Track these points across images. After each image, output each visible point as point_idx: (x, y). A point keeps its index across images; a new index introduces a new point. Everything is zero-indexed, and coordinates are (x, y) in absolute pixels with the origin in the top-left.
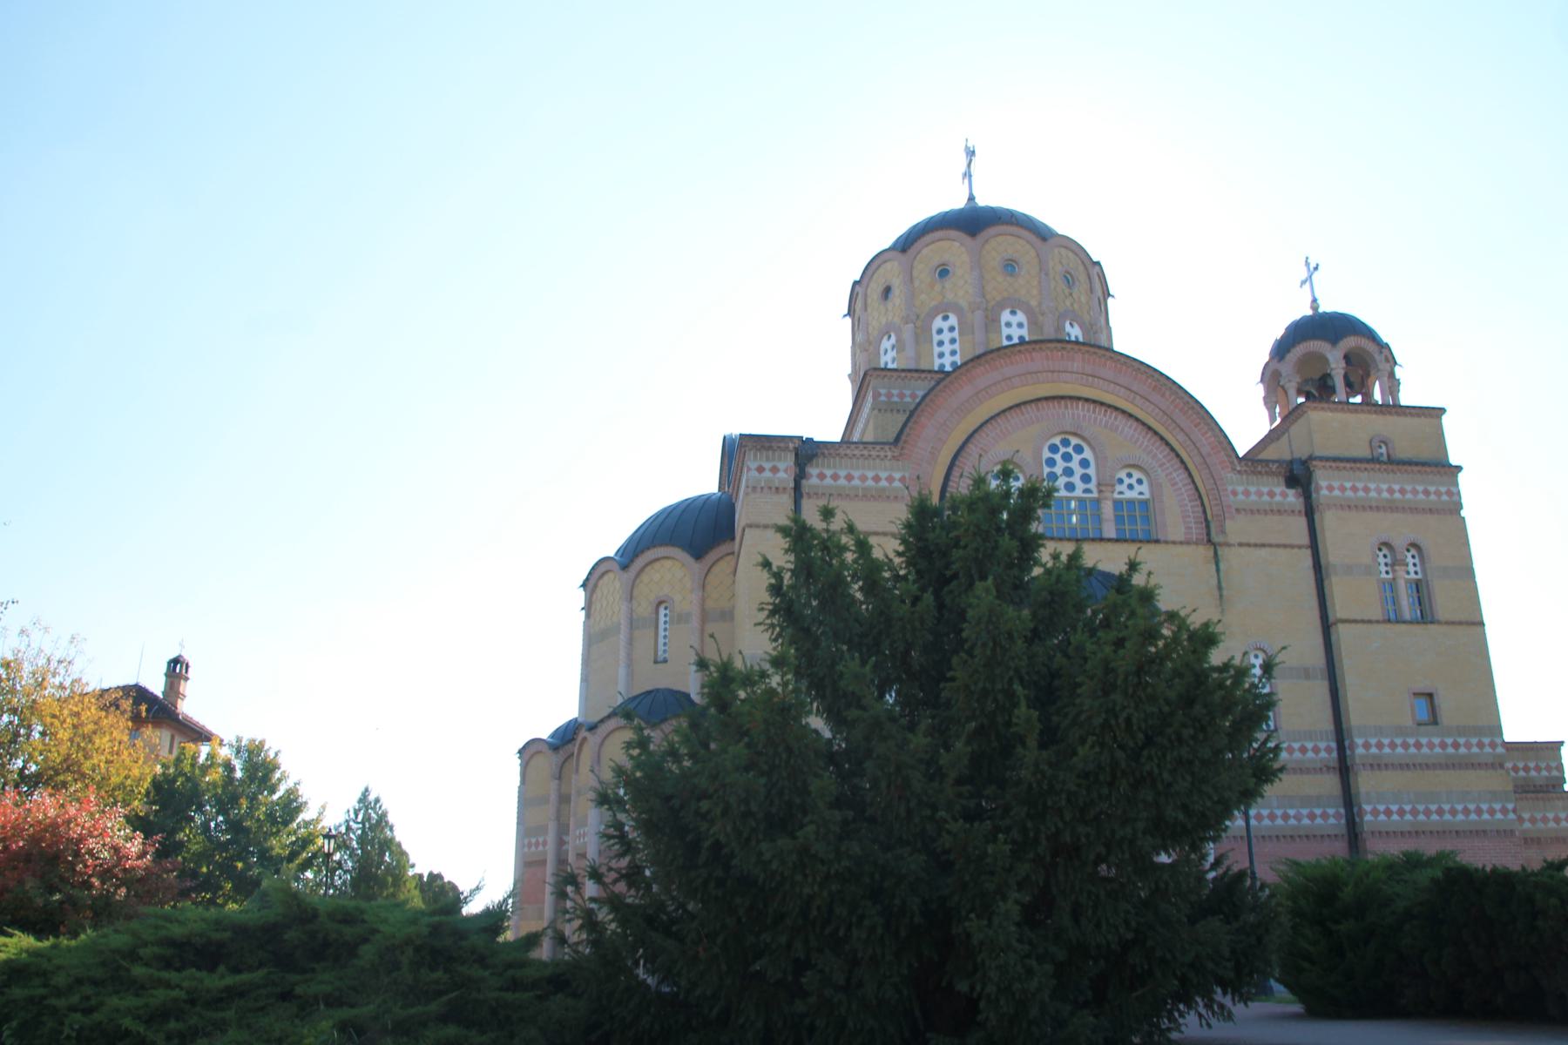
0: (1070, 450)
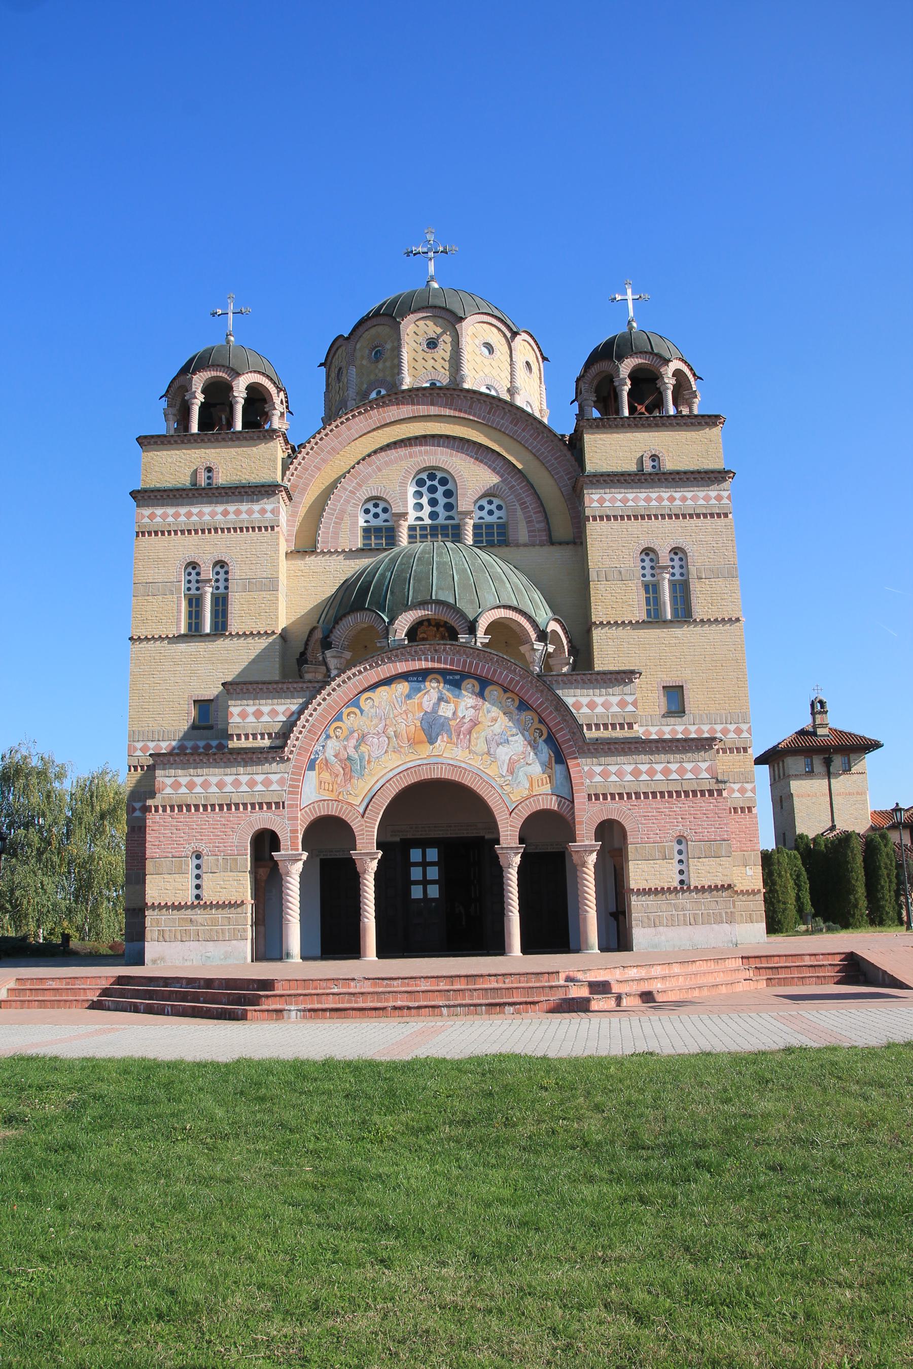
0: (436, 483)
